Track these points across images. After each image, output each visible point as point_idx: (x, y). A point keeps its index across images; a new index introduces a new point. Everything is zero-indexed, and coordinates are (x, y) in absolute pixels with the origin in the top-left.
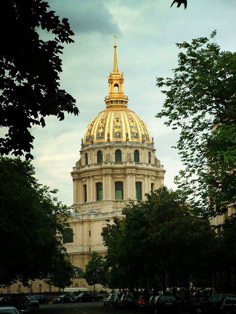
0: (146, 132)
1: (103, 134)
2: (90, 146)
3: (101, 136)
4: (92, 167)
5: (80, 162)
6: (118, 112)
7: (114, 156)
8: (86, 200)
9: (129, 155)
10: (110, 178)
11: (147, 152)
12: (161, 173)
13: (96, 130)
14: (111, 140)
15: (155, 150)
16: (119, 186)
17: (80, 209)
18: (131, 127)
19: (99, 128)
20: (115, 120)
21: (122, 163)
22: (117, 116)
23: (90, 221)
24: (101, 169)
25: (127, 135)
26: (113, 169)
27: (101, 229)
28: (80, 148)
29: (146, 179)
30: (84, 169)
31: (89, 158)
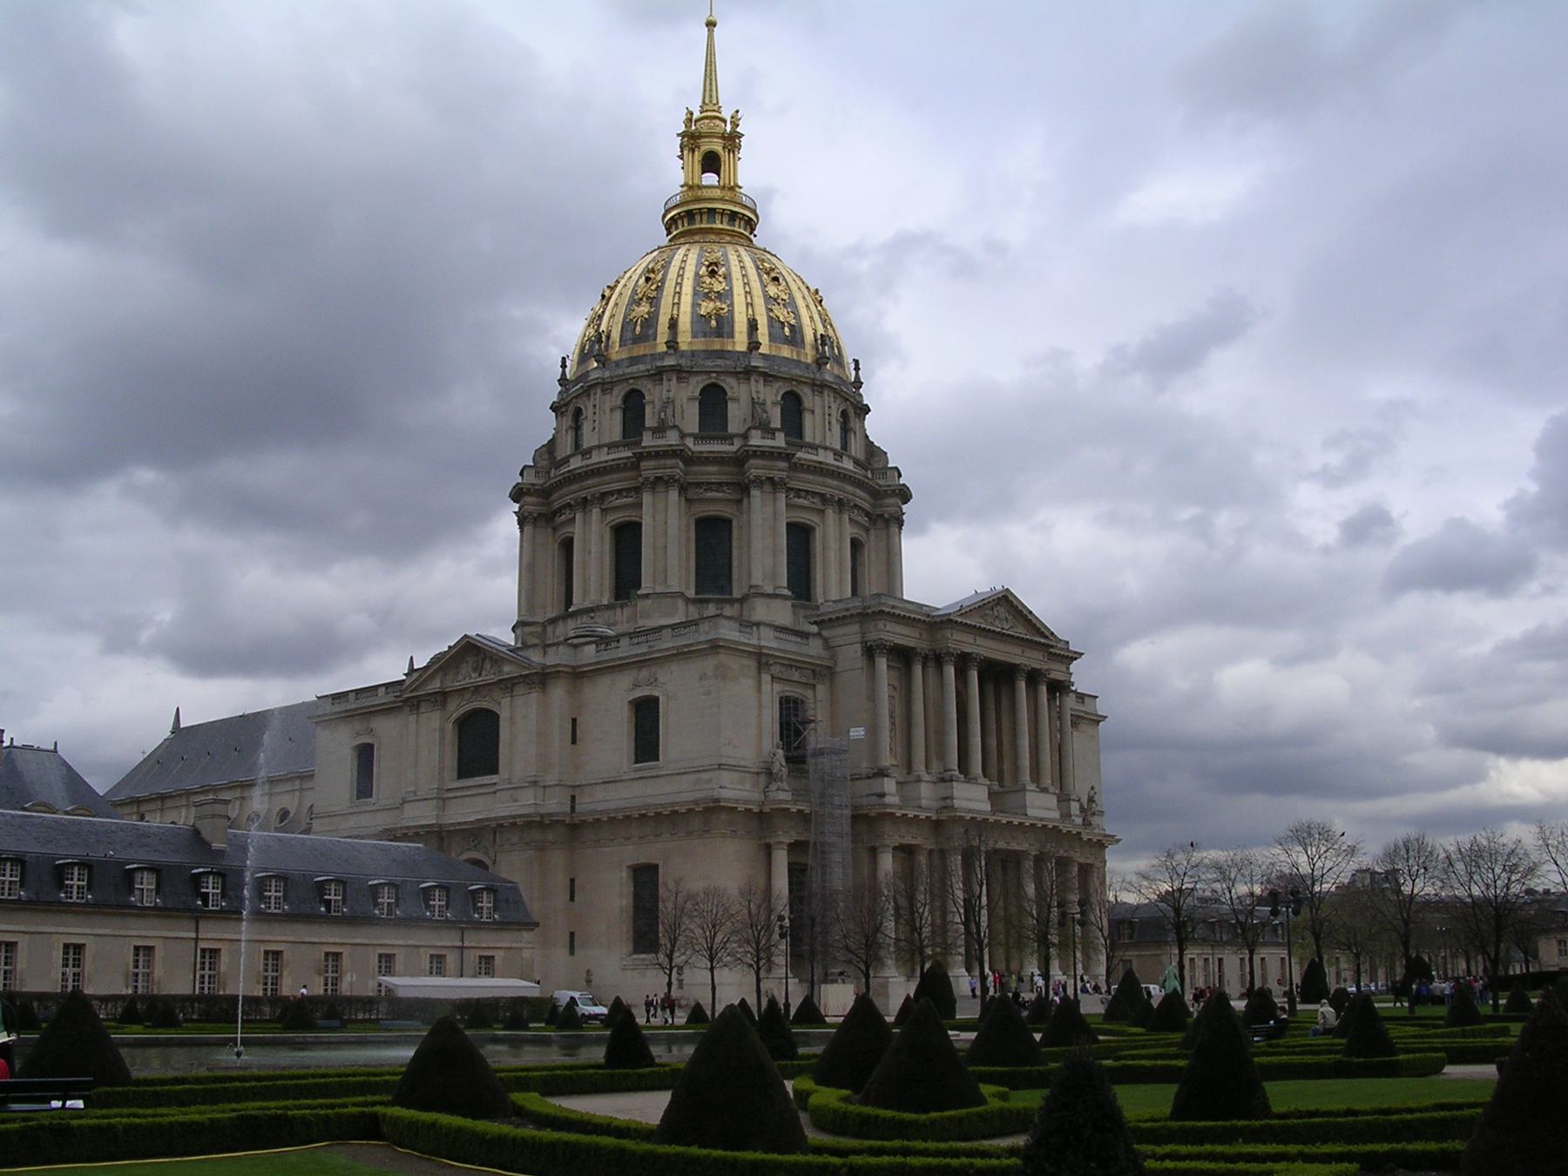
0: (831, 333)
1: (650, 322)
3: (639, 331)
5: (551, 446)
6: (715, 247)
8: (569, 601)
10: (674, 495)
11: (836, 409)
15: (867, 410)
16: (714, 543)
18: (769, 299)
19: (635, 301)
21: (730, 438)
23: (578, 675)
24: (634, 464)
25: (753, 326)
26: (690, 460)
27: (626, 707)
28: (553, 392)
29: (830, 512)
31: (586, 427)
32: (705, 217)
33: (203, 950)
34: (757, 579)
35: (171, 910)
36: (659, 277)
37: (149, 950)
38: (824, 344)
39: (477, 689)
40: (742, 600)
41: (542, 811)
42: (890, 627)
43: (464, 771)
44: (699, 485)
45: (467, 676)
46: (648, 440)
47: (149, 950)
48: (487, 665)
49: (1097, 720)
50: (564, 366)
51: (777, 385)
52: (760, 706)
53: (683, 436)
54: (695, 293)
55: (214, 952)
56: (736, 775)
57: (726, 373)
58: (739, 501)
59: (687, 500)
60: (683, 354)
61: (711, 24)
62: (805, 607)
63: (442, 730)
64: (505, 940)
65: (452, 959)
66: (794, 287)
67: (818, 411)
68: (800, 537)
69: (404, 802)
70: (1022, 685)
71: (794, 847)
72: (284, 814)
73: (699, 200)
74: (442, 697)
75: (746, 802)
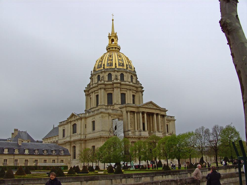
0: (129, 64)
1: (101, 65)
3: (99, 66)
4: (94, 85)
7: (107, 77)
9: (116, 76)
10: (103, 90)
11: (130, 75)
12: (139, 89)
14: (106, 67)
18: (118, 60)
19: (99, 62)
20: (109, 56)
21: (112, 81)
25: (116, 64)
26: (106, 85)
28: (90, 76)
32: (111, 48)
33: (15, 160)
35: (10, 154)
37: (6, 160)
39: (74, 120)
40: (113, 105)
41: (81, 138)
42: (130, 108)
44: (107, 88)
45: (73, 119)
46: (99, 82)
47: (6, 160)
48: (75, 117)
49: (174, 120)
50: (91, 72)
51: (119, 73)
53: (105, 81)
55: (17, 160)
57: (112, 71)
58: (114, 90)
59: (106, 91)
61: (113, 20)
63: (71, 127)
64: (65, 157)
65: (56, 161)
66: (123, 58)
67: (126, 76)
70: (155, 116)
73: (110, 46)
74: (71, 122)
75: (106, 136)
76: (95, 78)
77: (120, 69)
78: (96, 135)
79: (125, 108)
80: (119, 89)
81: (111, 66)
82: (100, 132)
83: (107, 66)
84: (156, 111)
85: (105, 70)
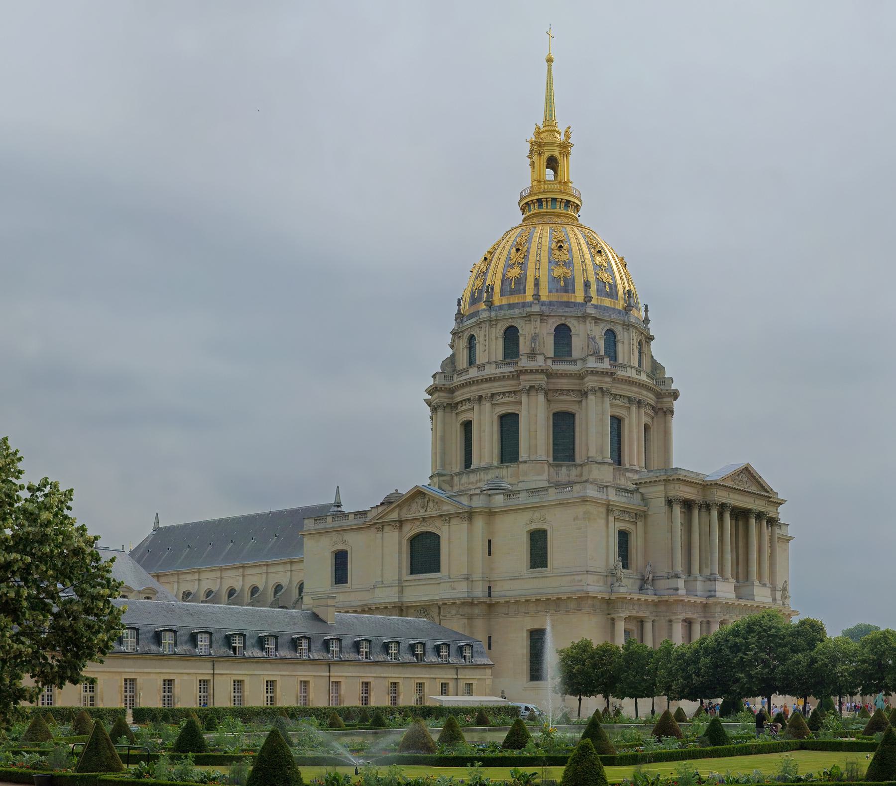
1: (520, 281)
2: (485, 315)
4: (490, 371)
5: (452, 359)
7: (550, 341)
10: (541, 398)
11: (636, 337)
13: (500, 271)
14: (544, 298)
16: (564, 426)
17: (452, 487)
21: (574, 361)
22: (560, 236)
23: (491, 514)
25: (587, 285)
26: (549, 374)
30: (465, 377)
31: (479, 349)
32: (549, 203)
34: (592, 453)
36: (525, 249)
38: (629, 296)
43: (414, 569)
45: (416, 510)
46: (524, 363)
48: (431, 504)
50: (459, 304)
51: (602, 325)
52: (608, 536)
54: (550, 262)
56: (595, 577)
57: (572, 316)
60: (543, 304)
62: (620, 470)
63: (400, 543)
67: (626, 342)
68: (617, 422)
69: (375, 587)
71: (627, 619)
72: (254, 590)
74: (401, 523)
76: (493, 336)
77: (606, 309)
78: (547, 583)
79: (662, 488)
80: (607, 400)
81: (566, 290)
82: (579, 578)
83: (550, 292)
84: (758, 502)
85: (544, 308)
